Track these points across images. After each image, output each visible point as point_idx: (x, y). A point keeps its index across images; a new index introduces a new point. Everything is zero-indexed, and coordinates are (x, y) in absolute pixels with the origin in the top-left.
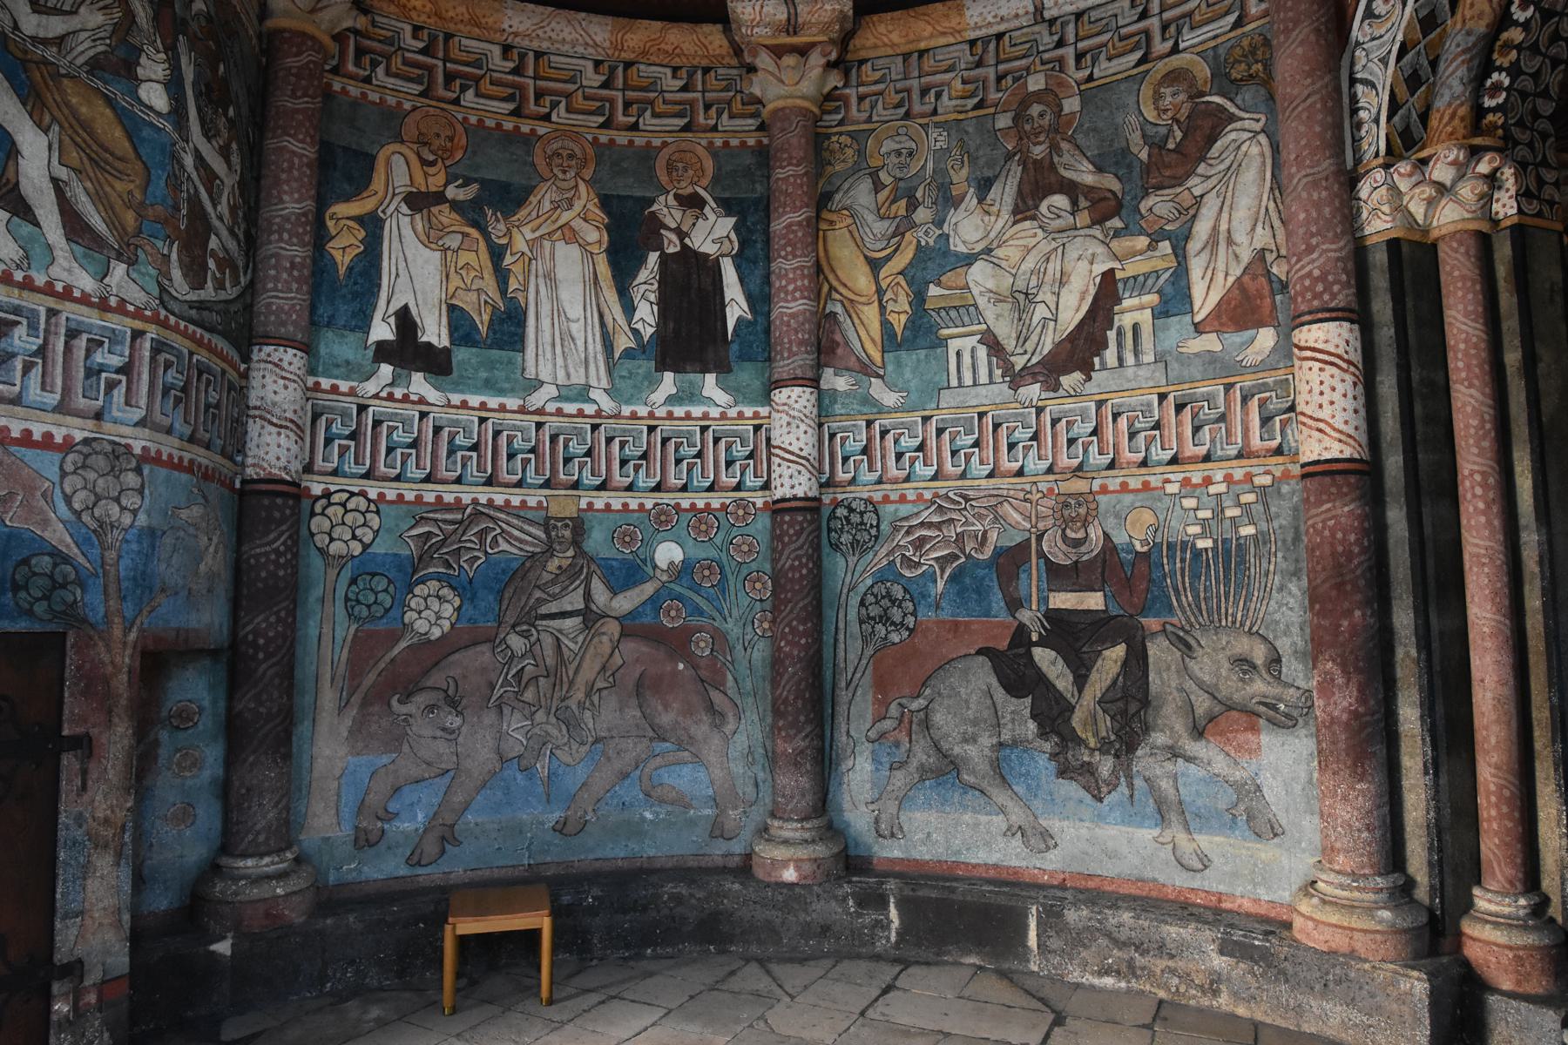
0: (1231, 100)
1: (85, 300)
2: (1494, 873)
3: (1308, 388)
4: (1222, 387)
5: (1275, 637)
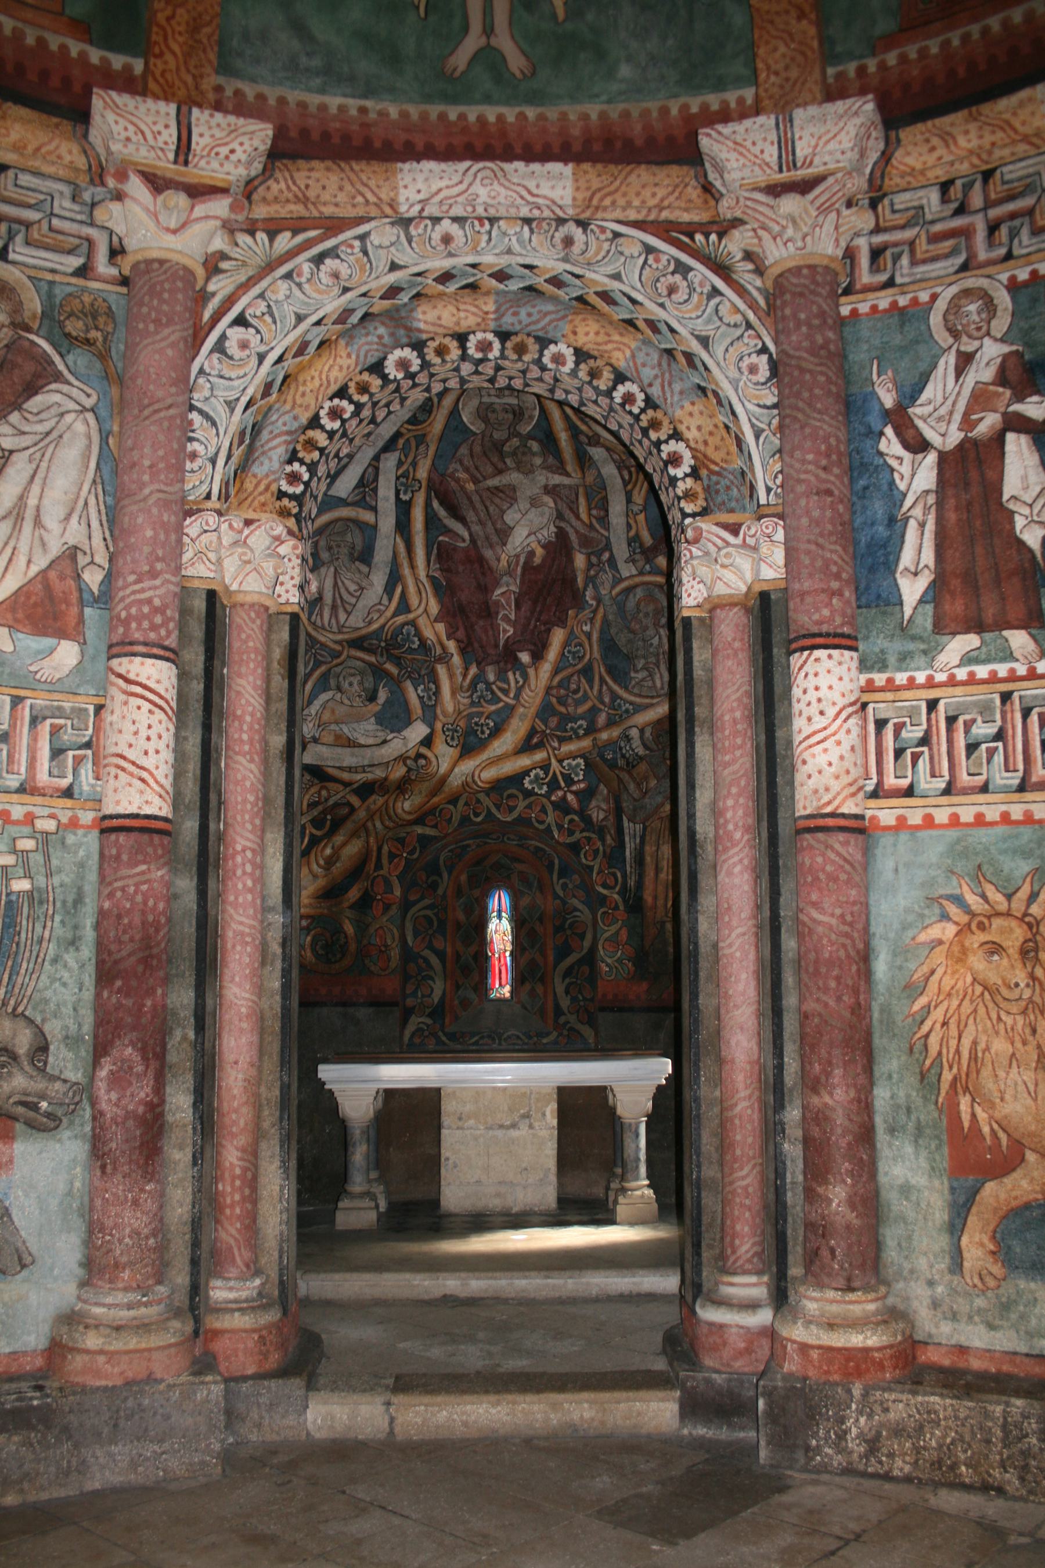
0: (62, 356)
2: (234, 1261)
3: (133, 728)
4: (8, 699)
5: (44, 1020)
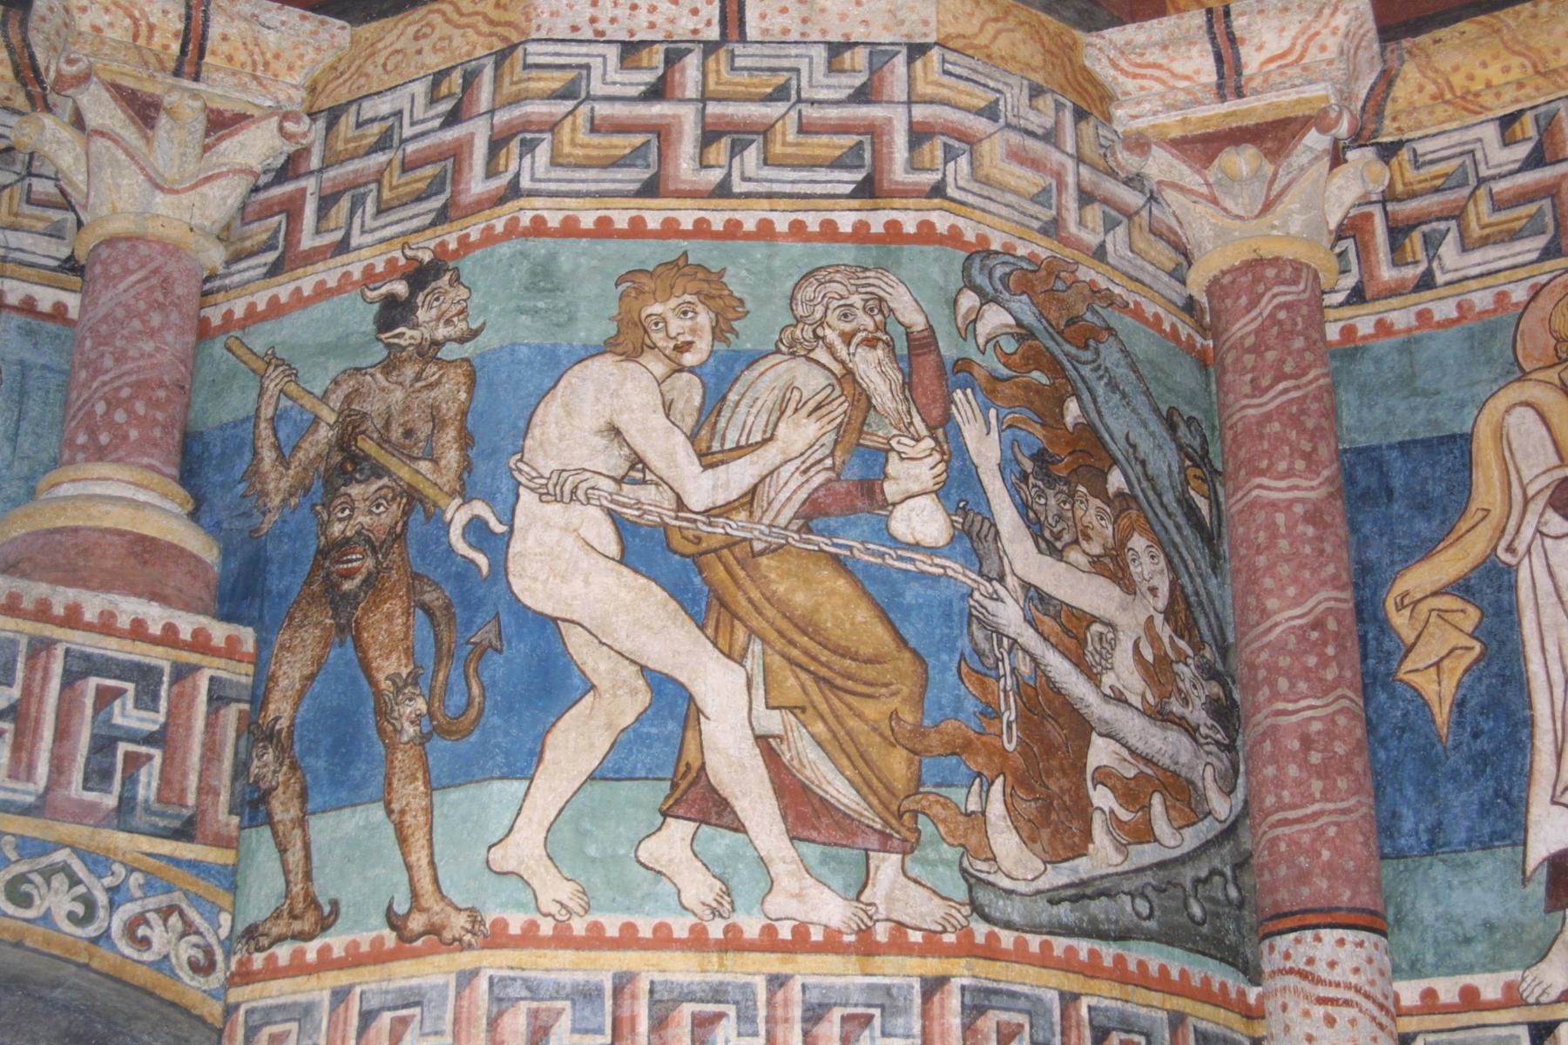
1: (832, 944)
